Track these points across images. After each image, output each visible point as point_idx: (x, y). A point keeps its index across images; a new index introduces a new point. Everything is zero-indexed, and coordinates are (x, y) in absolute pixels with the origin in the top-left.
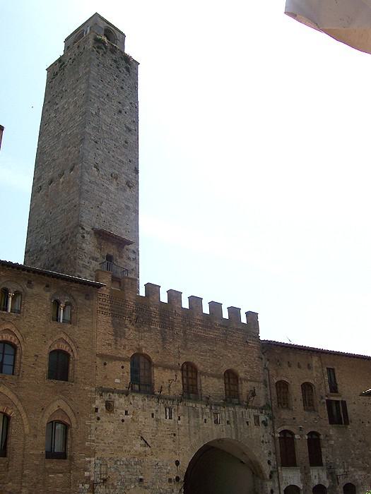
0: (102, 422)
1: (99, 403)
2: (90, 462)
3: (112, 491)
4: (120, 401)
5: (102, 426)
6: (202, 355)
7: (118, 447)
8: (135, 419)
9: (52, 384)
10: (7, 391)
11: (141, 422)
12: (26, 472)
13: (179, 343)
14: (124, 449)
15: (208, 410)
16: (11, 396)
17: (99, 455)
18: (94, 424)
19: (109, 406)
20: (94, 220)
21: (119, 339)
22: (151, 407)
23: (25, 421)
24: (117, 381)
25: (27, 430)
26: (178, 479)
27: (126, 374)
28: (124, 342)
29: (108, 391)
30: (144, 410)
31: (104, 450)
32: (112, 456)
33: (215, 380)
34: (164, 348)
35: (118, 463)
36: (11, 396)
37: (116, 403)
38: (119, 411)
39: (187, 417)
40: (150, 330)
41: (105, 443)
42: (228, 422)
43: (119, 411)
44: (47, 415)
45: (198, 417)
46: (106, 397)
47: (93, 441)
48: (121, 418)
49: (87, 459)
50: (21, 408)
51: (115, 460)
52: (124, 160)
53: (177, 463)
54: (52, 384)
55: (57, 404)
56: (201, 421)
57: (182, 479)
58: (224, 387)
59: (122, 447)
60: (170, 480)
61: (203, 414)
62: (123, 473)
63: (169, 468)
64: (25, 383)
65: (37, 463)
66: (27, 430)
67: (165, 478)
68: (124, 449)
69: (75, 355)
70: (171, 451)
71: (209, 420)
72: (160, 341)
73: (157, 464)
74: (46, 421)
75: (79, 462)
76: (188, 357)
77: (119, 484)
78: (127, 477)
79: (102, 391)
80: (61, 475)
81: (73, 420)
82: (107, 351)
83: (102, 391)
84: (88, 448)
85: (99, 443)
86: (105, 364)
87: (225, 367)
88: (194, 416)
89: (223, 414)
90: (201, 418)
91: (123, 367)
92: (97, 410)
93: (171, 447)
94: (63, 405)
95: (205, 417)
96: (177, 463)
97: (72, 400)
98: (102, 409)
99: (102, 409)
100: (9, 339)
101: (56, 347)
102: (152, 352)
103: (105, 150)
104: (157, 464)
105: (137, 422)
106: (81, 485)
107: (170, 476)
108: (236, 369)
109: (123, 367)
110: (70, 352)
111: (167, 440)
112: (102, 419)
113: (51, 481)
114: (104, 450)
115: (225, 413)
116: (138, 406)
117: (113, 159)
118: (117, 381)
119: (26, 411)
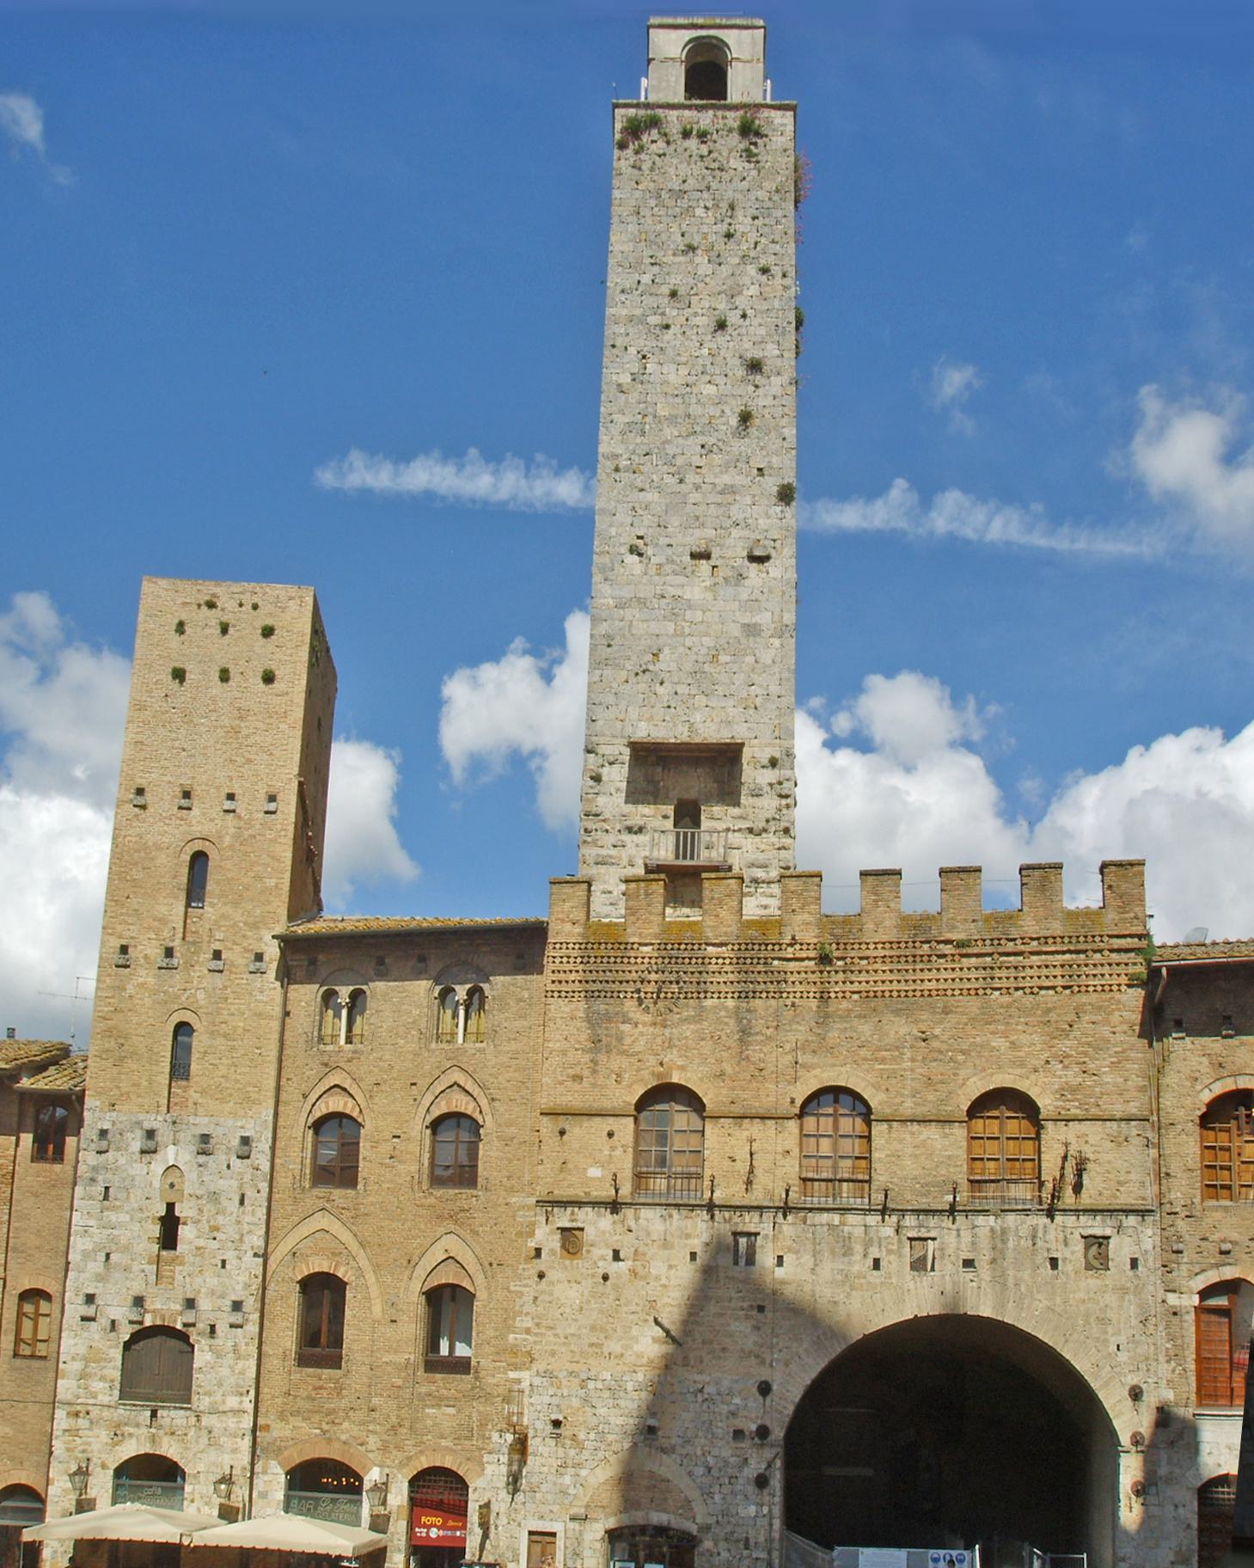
0: (552, 1283)
1: (546, 1236)
2: (519, 1381)
3: (572, 1452)
4: (597, 1226)
5: (551, 1294)
6: (883, 1061)
7: (591, 1345)
8: (639, 1270)
9: (431, 1200)
10: (336, 1227)
11: (657, 1278)
12: (375, 1401)
13: (799, 1032)
14: (606, 1351)
15: (888, 1231)
16: (345, 1236)
17: (539, 1366)
18: (530, 1287)
19: (570, 1238)
20: (634, 713)
21: (602, 1058)
22: (688, 1236)
23: (374, 1291)
24: (595, 1172)
25: (377, 1309)
26: (763, 1432)
27: (619, 1152)
28: (617, 1062)
29: (564, 1204)
30: (666, 1244)
31: (553, 1354)
32: (575, 1367)
33: (932, 1132)
34: (741, 1057)
35: (591, 1385)
36: (345, 1236)
37: (590, 1234)
38: (596, 1252)
39: (807, 1259)
40: (699, 1018)
41: (556, 1335)
42: (968, 1263)
43: (596, 1252)
44: (421, 1272)
45: (848, 1252)
46: (563, 1219)
47: (528, 1331)
48: (601, 1272)
49: (512, 1375)
50: (363, 1262)
51: (583, 1376)
52: (740, 480)
53: (765, 1389)
54: (431, 1200)
55: (444, 1251)
56: (860, 1265)
57: (778, 1433)
58: (963, 1155)
59: (600, 1346)
60: (738, 1434)
61: (868, 1244)
62: (601, 1411)
63: (737, 1400)
64: (372, 1204)
65: (399, 1382)
66: (377, 1309)
67: (723, 1428)
68: (606, 1351)
69: (489, 1124)
70: (745, 1354)
71: (890, 1263)
72: (733, 1042)
73: (701, 1391)
74: (416, 1287)
75: (491, 1380)
76: (825, 1075)
77: (592, 1436)
78: (612, 1420)
79: (552, 1203)
80: (451, 1411)
81: (480, 1279)
82: (570, 1097)
83: (552, 1203)
84: (514, 1351)
85: (542, 1334)
86: (562, 1133)
87: (977, 1087)
88: (833, 1252)
89: (951, 1239)
90: (857, 1257)
91: (610, 1135)
92: (538, 1252)
93: (749, 1345)
94: (452, 1244)
95: (874, 1252)
96: (765, 1389)
97: (477, 1233)
98: (553, 1252)
99: (553, 1252)
100: (340, 1109)
101: (442, 1108)
102: (701, 1079)
103: (669, 479)
104: (701, 1391)
105: (644, 1278)
106: (495, 1436)
107: (739, 1423)
108: (1022, 1086)
109: (610, 1135)
110: (477, 1116)
111: (735, 1326)
112: (550, 1275)
113: (429, 1422)
114: (553, 1354)
115: (952, 1238)
116: (648, 1234)
117: (695, 497)
118: (595, 1172)
119: (377, 1268)
